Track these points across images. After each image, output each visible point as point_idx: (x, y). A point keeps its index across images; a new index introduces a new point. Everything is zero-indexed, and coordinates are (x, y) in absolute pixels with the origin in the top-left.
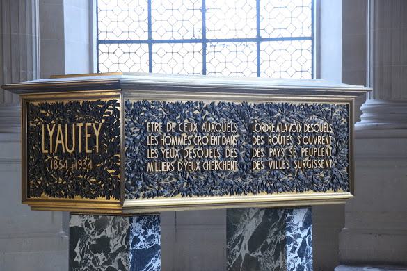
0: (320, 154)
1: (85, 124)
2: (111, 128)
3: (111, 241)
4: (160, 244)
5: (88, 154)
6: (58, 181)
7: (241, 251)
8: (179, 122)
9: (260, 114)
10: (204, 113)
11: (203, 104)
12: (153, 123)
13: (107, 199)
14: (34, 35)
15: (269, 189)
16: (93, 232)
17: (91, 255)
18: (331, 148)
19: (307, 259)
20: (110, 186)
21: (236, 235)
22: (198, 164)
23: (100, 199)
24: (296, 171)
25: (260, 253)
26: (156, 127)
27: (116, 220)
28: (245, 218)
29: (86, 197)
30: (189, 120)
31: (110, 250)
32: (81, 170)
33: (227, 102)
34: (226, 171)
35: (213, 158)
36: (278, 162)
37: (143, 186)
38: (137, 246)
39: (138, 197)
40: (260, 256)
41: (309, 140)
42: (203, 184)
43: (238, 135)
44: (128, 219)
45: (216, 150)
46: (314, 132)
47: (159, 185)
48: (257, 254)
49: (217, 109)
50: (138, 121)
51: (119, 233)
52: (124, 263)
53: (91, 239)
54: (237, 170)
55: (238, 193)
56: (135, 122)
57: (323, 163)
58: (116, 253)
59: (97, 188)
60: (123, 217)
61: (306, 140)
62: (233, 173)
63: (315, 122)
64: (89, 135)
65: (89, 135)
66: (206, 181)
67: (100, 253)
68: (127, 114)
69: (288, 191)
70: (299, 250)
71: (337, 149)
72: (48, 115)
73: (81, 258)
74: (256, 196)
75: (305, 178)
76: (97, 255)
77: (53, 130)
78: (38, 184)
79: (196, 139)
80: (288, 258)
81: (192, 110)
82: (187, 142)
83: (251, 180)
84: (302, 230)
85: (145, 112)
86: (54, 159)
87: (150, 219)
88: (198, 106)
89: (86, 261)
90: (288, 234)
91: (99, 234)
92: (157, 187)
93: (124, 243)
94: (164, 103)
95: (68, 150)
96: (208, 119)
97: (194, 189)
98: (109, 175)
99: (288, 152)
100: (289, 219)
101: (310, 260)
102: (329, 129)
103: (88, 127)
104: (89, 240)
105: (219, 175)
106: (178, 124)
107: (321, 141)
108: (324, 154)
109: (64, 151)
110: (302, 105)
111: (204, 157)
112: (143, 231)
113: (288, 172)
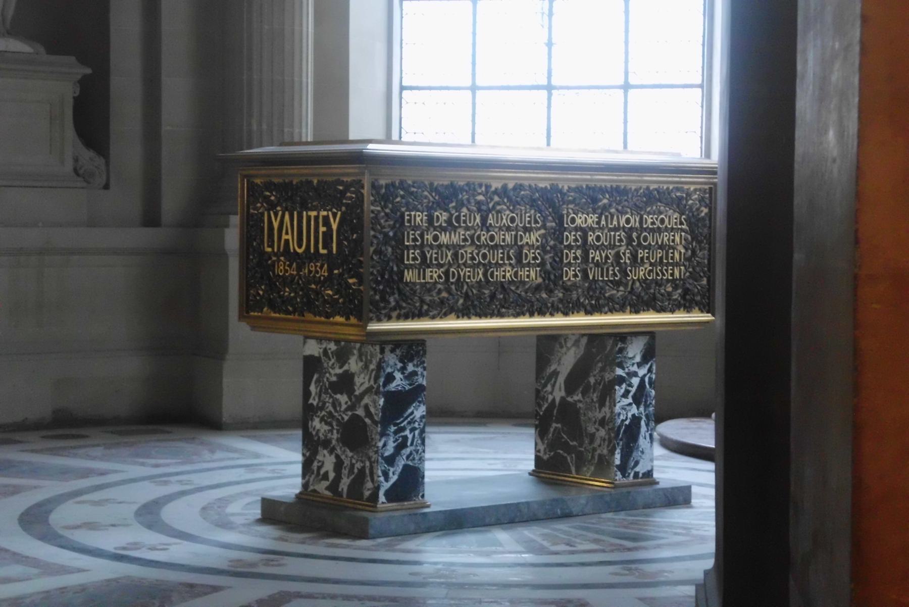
0: (667, 258)
2: (353, 221)
4: (424, 383)
5: (322, 255)
6: (285, 292)
7: (554, 394)
8: (453, 212)
9: (577, 202)
10: (492, 199)
11: (490, 186)
12: (413, 213)
14: (304, 80)
15: (588, 308)
16: (333, 364)
18: (683, 251)
19: (646, 406)
20: (351, 301)
22: (480, 273)
23: (338, 319)
24: (630, 283)
25: (580, 395)
26: (418, 219)
27: (363, 350)
28: (562, 347)
29: (320, 316)
30: (469, 210)
31: (355, 391)
32: (314, 276)
33: (526, 183)
34: (523, 283)
35: (504, 264)
36: (602, 269)
37: (397, 302)
38: (392, 387)
39: (389, 318)
40: (580, 401)
41: (650, 238)
42: (488, 300)
43: (543, 231)
44: (378, 348)
45: (508, 252)
46: (659, 228)
47: (422, 301)
48: (576, 398)
49: (511, 193)
50: (391, 210)
51: (366, 367)
52: (372, 410)
53: (330, 374)
54: (540, 280)
55: (542, 313)
56: (387, 211)
57: (670, 272)
59: (333, 303)
60: (372, 345)
61: (645, 239)
62: (534, 285)
63: (661, 213)
64: (324, 229)
65: (324, 229)
66: (493, 296)
67: (342, 394)
68: (375, 201)
69: (616, 311)
70: (635, 394)
71: (694, 253)
72: (273, 198)
73: (317, 400)
74: (568, 318)
75: (643, 294)
76: (338, 396)
77: (279, 219)
78: (259, 294)
79: (479, 238)
80: (618, 405)
81: (474, 196)
82: (465, 240)
83: (561, 295)
84: (639, 365)
85: (403, 197)
86: (279, 261)
87: (412, 348)
88: (483, 189)
89: (324, 403)
90: (619, 372)
91: (341, 367)
92: (418, 304)
93: (372, 382)
94: (431, 184)
96: (498, 208)
97: (474, 307)
98: (348, 286)
99: (617, 256)
100: (621, 350)
101: (651, 409)
102: (681, 223)
103: (324, 217)
104: (327, 375)
105: (513, 288)
106: (452, 215)
107: (668, 240)
108: (672, 258)
110: (641, 188)
111: (489, 262)
112: (400, 365)
113: (617, 284)
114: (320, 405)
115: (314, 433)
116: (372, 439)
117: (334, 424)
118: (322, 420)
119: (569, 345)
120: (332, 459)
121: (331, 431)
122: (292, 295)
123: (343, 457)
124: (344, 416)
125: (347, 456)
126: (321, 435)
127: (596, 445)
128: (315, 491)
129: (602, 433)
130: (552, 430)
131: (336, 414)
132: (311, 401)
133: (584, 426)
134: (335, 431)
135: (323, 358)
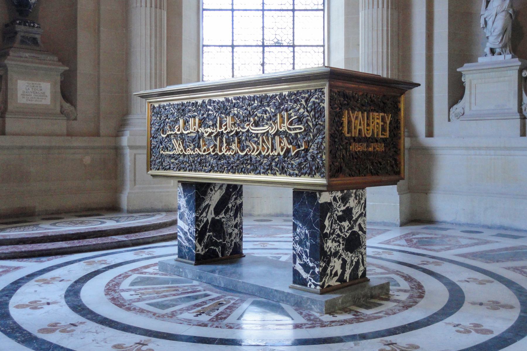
3: (353, 209)
16: (340, 205)
17: (338, 225)
21: (204, 205)
25: (223, 214)
27: (357, 193)
28: (211, 190)
40: (223, 218)
48: (221, 216)
51: (359, 202)
58: (357, 220)
67: (345, 221)
73: (330, 229)
76: (343, 223)
89: (334, 230)
91: (344, 206)
93: (362, 210)
95: (367, 135)
114: (332, 231)
115: (328, 250)
117: (341, 240)
118: (333, 240)
119: (216, 189)
120: (341, 261)
121: (339, 245)
124: (347, 234)
125: (349, 257)
127: (233, 238)
128: (329, 286)
129: (236, 231)
130: (206, 237)
133: (225, 229)
134: (341, 245)
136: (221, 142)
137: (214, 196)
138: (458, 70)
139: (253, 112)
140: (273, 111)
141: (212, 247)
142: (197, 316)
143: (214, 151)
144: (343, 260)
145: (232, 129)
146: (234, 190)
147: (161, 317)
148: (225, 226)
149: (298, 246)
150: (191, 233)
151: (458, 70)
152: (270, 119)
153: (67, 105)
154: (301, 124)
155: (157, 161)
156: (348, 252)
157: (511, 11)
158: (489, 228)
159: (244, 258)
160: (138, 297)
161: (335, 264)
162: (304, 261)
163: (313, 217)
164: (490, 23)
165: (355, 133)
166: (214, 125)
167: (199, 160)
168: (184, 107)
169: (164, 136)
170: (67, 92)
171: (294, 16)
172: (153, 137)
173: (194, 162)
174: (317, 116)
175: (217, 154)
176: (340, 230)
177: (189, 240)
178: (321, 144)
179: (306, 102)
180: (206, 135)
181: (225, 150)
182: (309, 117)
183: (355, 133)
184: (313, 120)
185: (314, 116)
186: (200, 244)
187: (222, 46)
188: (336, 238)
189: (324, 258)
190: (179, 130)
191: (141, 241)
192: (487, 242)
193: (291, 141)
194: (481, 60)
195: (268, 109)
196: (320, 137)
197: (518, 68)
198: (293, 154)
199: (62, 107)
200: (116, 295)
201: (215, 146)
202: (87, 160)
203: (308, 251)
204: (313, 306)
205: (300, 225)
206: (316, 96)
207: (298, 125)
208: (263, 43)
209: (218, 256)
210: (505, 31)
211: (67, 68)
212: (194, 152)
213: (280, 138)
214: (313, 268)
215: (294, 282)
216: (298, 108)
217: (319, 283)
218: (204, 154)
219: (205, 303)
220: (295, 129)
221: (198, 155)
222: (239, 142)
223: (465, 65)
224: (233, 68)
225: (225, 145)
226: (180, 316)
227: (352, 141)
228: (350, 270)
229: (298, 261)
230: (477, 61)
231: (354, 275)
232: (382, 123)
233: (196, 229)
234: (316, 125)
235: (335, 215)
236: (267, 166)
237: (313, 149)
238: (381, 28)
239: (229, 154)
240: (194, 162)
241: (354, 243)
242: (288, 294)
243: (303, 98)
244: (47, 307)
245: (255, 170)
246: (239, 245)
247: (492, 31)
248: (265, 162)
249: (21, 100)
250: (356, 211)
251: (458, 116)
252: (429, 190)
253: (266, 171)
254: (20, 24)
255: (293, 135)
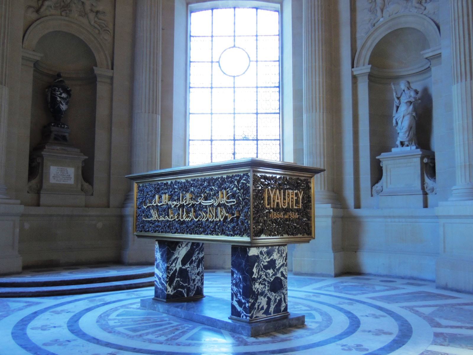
1: (293, 191)
3: (277, 262)
6: (273, 226)
13: (303, 235)
16: (265, 257)
17: (264, 272)
25: (189, 265)
27: (280, 249)
28: (180, 247)
31: (276, 267)
40: (188, 267)
48: (186, 266)
51: (281, 255)
53: (264, 262)
58: (279, 268)
65: (296, 198)
67: (270, 269)
73: (257, 275)
76: (268, 271)
77: (273, 193)
89: (261, 276)
103: (296, 193)
109: (281, 207)
115: (256, 290)
116: (285, 285)
117: (266, 283)
118: (260, 283)
119: (183, 246)
120: (266, 299)
122: (277, 227)
123: (271, 297)
124: (271, 279)
125: (273, 296)
126: (259, 290)
127: (195, 283)
128: (257, 317)
129: (198, 277)
130: (175, 282)
131: (267, 279)
132: (254, 276)
133: (190, 276)
134: (267, 287)
135: (260, 256)
136: (183, 211)
137: (181, 251)
138: (377, 158)
139: (204, 190)
140: (217, 189)
141: (180, 289)
142: (158, 337)
143: (178, 218)
144: (268, 298)
145: (190, 202)
146: (196, 246)
147: (132, 337)
148: (189, 274)
149: (235, 287)
150: (163, 279)
151: (377, 158)
152: (214, 195)
153: (86, 185)
154: (235, 198)
155: (141, 225)
156: (273, 293)
157: (414, 114)
158: (403, 278)
159: (204, 298)
160: (119, 324)
161: (262, 301)
162: (238, 299)
163: (245, 266)
164: (399, 123)
165: (274, 205)
166: (178, 199)
167: (168, 225)
168: (159, 186)
169: (145, 207)
170: (87, 174)
171: (257, 118)
172: (138, 208)
173: (165, 226)
174: (245, 193)
175: (180, 220)
176: (266, 275)
177: (162, 284)
178: (248, 212)
179: (238, 182)
180: (173, 206)
181: (185, 217)
182: (240, 193)
183: (274, 205)
184: (242, 195)
185: (243, 193)
186: (170, 286)
187: (203, 140)
188: (263, 282)
189: (252, 296)
190: (155, 203)
191: (134, 286)
192: (397, 289)
193: (228, 210)
194: (393, 150)
195: (213, 187)
196: (247, 207)
197: (420, 156)
198: (229, 220)
199: (82, 186)
200: (104, 323)
201: (179, 214)
202: (100, 225)
203: (241, 291)
204: (243, 332)
205: (236, 272)
206: (244, 178)
207: (233, 199)
208: (234, 137)
209: (184, 296)
210: (410, 128)
211: (87, 157)
212: (165, 218)
213: (221, 208)
214: (245, 303)
215: (232, 314)
216: (232, 187)
217: (248, 315)
218: (171, 220)
219: (166, 328)
220: (231, 202)
221: (168, 221)
222: (194, 212)
223: (382, 154)
224: (211, 157)
225: (185, 213)
226: (146, 337)
227: (271, 211)
228: (274, 306)
229: (235, 299)
230: (390, 151)
231: (277, 310)
232: (296, 198)
233: (167, 275)
234: (244, 199)
235: (261, 265)
236: (212, 229)
237: (242, 216)
238: (318, 127)
239: (187, 220)
240: (165, 226)
241: (277, 286)
242: (227, 322)
243: (236, 180)
244: (53, 330)
245: (204, 232)
246: (200, 288)
247: (401, 128)
248: (211, 226)
249: (52, 181)
250: (279, 262)
251: (378, 193)
252: (358, 249)
253: (212, 232)
254: (54, 126)
255: (229, 206)
